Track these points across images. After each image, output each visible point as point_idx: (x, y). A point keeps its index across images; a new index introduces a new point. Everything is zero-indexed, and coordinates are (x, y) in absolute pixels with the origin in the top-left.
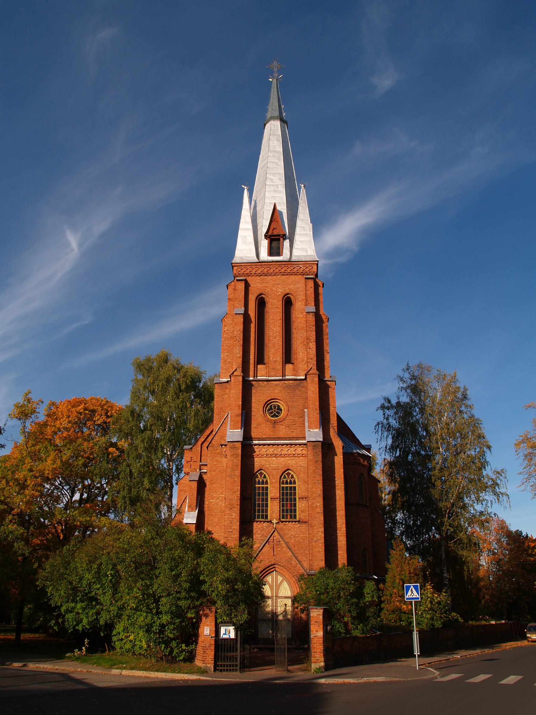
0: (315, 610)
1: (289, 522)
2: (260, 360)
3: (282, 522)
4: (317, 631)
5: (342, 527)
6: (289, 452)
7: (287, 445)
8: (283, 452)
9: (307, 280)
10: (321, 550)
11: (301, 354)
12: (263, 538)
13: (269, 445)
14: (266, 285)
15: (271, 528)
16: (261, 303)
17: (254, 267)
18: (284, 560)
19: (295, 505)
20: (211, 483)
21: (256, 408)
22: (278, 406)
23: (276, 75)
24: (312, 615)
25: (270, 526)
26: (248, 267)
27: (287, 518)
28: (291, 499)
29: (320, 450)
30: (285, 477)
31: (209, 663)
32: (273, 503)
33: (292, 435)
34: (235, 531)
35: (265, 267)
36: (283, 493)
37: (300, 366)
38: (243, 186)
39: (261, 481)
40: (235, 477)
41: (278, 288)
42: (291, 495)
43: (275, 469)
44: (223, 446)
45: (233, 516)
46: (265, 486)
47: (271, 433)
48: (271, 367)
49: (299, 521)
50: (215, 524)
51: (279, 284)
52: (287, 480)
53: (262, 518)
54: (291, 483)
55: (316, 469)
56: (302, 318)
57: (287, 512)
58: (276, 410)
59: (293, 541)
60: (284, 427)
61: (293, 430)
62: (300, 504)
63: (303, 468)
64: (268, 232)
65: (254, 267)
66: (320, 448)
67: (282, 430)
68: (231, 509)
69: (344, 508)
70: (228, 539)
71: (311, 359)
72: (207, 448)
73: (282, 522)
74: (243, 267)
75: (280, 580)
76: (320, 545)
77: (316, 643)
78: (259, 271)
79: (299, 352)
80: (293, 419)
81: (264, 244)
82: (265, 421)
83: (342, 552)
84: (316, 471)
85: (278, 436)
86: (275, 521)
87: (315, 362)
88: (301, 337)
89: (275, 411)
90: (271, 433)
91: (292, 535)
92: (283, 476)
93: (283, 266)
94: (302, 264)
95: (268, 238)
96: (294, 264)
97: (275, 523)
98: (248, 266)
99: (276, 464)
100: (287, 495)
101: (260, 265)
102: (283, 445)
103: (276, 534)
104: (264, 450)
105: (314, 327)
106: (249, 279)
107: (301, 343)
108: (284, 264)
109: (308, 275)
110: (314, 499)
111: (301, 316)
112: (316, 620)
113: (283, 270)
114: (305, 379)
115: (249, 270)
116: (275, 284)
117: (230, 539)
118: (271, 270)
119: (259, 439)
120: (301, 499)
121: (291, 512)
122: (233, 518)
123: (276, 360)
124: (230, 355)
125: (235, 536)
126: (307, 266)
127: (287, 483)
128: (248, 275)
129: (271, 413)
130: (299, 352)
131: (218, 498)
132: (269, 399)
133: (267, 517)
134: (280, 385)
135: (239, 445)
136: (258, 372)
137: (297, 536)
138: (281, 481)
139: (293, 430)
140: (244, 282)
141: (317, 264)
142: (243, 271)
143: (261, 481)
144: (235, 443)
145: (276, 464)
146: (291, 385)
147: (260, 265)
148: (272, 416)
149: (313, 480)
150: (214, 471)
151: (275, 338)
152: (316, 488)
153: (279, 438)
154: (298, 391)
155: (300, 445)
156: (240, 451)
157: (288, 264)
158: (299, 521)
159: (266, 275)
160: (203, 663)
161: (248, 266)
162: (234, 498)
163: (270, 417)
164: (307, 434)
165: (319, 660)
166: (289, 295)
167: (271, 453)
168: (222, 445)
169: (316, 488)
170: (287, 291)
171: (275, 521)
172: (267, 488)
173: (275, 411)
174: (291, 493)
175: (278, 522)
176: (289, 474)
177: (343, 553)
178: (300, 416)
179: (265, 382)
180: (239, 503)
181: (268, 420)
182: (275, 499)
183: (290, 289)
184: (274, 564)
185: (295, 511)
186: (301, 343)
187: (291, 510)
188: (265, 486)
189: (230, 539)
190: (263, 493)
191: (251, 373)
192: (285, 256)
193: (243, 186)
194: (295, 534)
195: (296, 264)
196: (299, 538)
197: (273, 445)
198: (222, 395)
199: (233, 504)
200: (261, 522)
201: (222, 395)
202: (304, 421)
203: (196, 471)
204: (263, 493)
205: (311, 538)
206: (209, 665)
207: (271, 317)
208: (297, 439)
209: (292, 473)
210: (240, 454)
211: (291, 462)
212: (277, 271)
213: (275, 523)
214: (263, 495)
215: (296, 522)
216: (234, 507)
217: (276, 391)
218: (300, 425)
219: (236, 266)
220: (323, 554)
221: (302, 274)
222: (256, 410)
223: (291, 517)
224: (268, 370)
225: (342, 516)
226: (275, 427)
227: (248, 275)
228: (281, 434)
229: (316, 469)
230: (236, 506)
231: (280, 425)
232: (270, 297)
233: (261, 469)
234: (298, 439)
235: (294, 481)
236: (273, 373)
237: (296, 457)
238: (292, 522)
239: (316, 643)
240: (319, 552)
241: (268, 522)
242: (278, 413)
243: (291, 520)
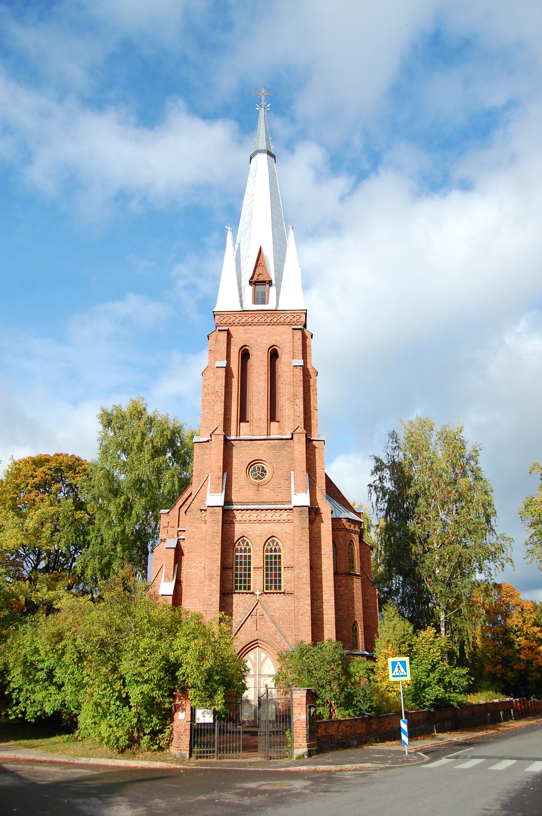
0: (298, 692)
1: (274, 593)
2: (243, 418)
3: (266, 593)
4: (300, 714)
5: (330, 598)
6: (274, 518)
7: (272, 510)
8: (267, 518)
9: (294, 331)
10: (307, 624)
11: (287, 410)
12: (245, 611)
13: (252, 510)
14: (250, 335)
15: (254, 600)
16: (245, 355)
17: (237, 316)
18: (268, 635)
19: (280, 575)
20: (189, 552)
21: (238, 469)
22: (263, 467)
23: (263, 103)
24: (294, 696)
25: (253, 598)
26: (231, 316)
27: (271, 589)
28: (275, 568)
29: (308, 516)
30: (269, 545)
31: (184, 750)
32: (256, 573)
33: (277, 499)
34: (214, 604)
35: (250, 316)
36: (267, 562)
37: (287, 424)
38: (227, 227)
39: (243, 549)
40: (215, 544)
41: (263, 339)
42: (275, 564)
43: (258, 536)
44: (203, 512)
45: (212, 587)
46: (247, 554)
47: (255, 497)
48: (255, 425)
49: (284, 593)
50: (193, 596)
51: (264, 335)
52: (271, 548)
53: (245, 589)
54: (275, 551)
55: (303, 536)
56: (289, 372)
57: (271, 582)
59: (277, 614)
60: (269, 490)
61: (278, 494)
62: (285, 574)
63: (289, 534)
64: (252, 278)
65: (237, 316)
66: (307, 513)
67: (267, 494)
68: (211, 579)
69: (333, 579)
70: (207, 612)
71: (298, 417)
72: (185, 513)
73: (266, 593)
74: (225, 316)
75: (264, 657)
76: (307, 618)
77: (299, 727)
78: (243, 321)
79: (285, 409)
80: (278, 481)
81: (248, 290)
82: (248, 484)
84: (303, 538)
86: (258, 593)
87: (303, 420)
88: (288, 392)
89: (259, 473)
90: (255, 497)
91: (276, 608)
92: (267, 544)
93: (269, 315)
94: (289, 313)
95: (253, 284)
96: (280, 313)
97: (258, 595)
98: (231, 314)
99: (259, 531)
100: (271, 564)
101: (244, 314)
102: (267, 510)
103: (258, 606)
104: (247, 514)
105: (302, 382)
106: (232, 329)
107: (288, 399)
108: (270, 313)
109: (296, 325)
110: (300, 569)
111: (289, 370)
112: (298, 702)
113: (269, 320)
114: (292, 439)
115: (231, 320)
116: (260, 335)
117: (210, 612)
118: (256, 320)
119: (242, 503)
120: (286, 568)
121: (275, 582)
122: (212, 590)
123: (260, 418)
124: (211, 411)
125: (215, 609)
126: (295, 315)
127: (271, 551)
128: (231, 325)
129: (256, 474)
130: (285, 409)
131: (197, 568)
132: (252, 460)
133: (249, 588)
134: (265, 445)
135: (220, 510)
136: (241, 430)
137: (282, 609)
138: (265, 549)
139: (278, 494)
140: (226, 332)
141: (306, 314)
142: (225, 320)
143: (243, 549)
144: (216, 508)
145: (259, 531)
146: (276, 444)
147: (244, 314)
148: (256, 479)
149: (299, 548)
150: (193, 538)
151: (259, 394)
152: (302, 557)
153: (263, 502)
154: (283, 451)
155: (286, 510)
156: (221, 517)
157: (274, 313)
158: (284, 593)
159: (250, 325)
160: (178, 750)
161: (231, 314)
162: (214, 568)
163: (253, 479)
164: (293, 496)
165: (301, 745)
166: (275, 347)
167: (255, 518)
168: (201, 510)
169: (302, 557)
170: (273, 343)
171: (258, 593)
172: (250, 556)
173: (259, 473)
174: (275, 562)
175: (262, 594)
176: (273, 541)
177: (331, 628)
178: (286, 478)
179: (249, 442)
180: (219, 574)
181: (251, 483)
182: (258, 568)
183: (276, 341)
184: (257, 640)
185: (280, 581)
186: (288, 399)
187: (275, 580)
188: (247, 554)
189: (210, 612)
190: (245, 562)
191: (233, 431)
192: (271, 305)
193: (227, 227)
195: (283, 313)
196: (284, 611)
197: (257, 510)
198: (202, 455)
199: (213, 575)
200: (243, 593)
201: (202, 455)
202: (290, 483)
203: (173, 537)
204: (245, 562)
205: (297, 612)
206: (184, 752)
207: (255, 371)
208: (283, 503)
209: (277, 540)
210: (221, 519)
211: (275, 529)
212: (262, 320)
213: (258, 595)
214: (245, 564)
215: (281, 593)
216: (213, 578)
217: (261, 451)
218: (286, 489)
219: (218, 315)
220: (309, 628)
221: (289, 324)
222: (238, 472)
223: (276, 588)
224: (251, 428)
225: (330, 587)
226: (259, 490)
227: (231, 325)
228: (265, 498)
229: (303, 536)
230: (216, 576)
232: (254, 349)
233: (243, 536)
234: (284, 503)
235: (279, 548)
236: (256, 432)
237: (281, 523)
238: (277, 593)
239: (299, 727)
240: (305, 626)
241: (251, 593)
242: (262, 475)
243: (276, 591)
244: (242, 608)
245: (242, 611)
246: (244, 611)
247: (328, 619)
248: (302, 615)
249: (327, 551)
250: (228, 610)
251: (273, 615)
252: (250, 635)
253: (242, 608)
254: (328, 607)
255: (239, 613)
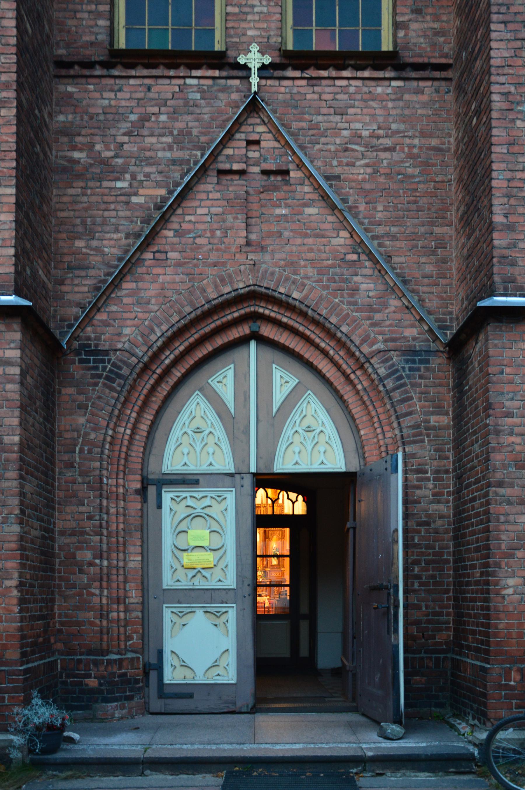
12: (184, 155)
15: (235, 96)
75: (287, 389)
91: (357, 136)
137: (387, 142)
194: (372, 136)
196: (396, 156)
244: (169, 140)
245: (168, 154)
246: (178, 154)
250: (91, 146)
251: (337, 171)
252: (212, 272)
253: (169, 140)
255: (151, 161)
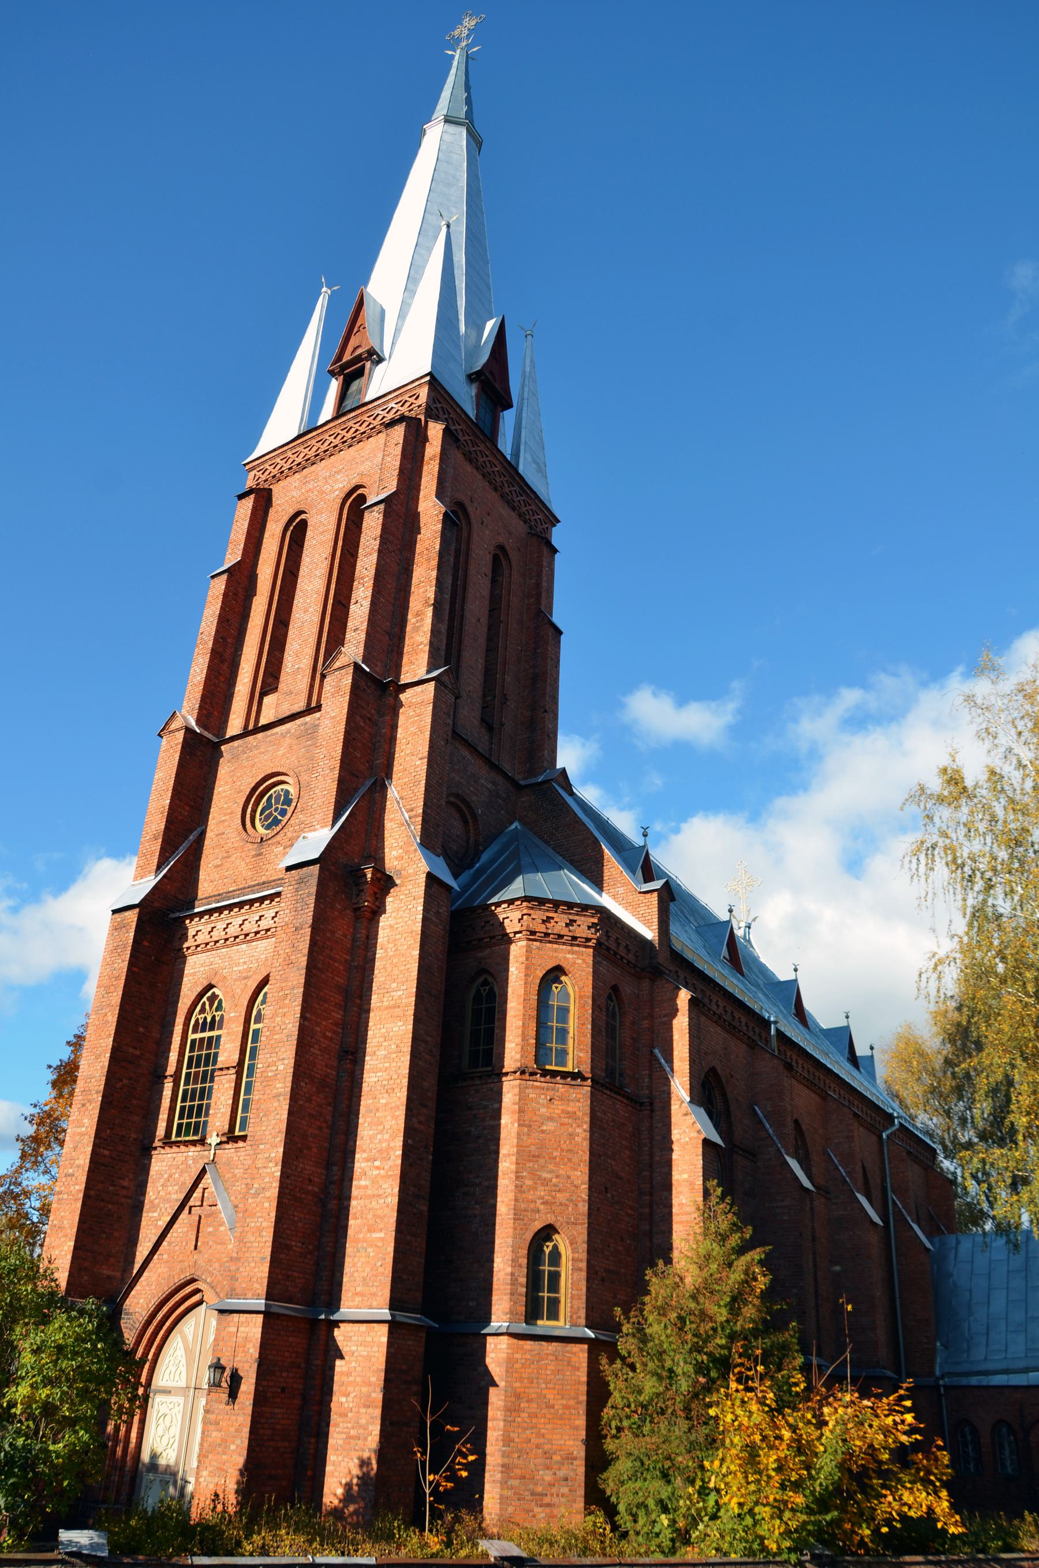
5: (392, 1144)
10: (265, 1224)
17: (289, 454)
58: (279, 806)
70: (60, 1196)
76: (266, 1205)
83: (382, 1235)
85: (264, 879)
99: (245, 963)
103: (208, 1180)
123: (298, 668)
143: (209, 1020)
170: (354, 482)
184: (193, 1281)
195: (379, 406)
220: (268, 1236)
222: (227, 817)
226: (261, 854)
231: (272, 844)
247: (379, 1212)
248: (256, 1195)
249: (400, 997)
253: (176, 1188)
254: (382, 1172)
